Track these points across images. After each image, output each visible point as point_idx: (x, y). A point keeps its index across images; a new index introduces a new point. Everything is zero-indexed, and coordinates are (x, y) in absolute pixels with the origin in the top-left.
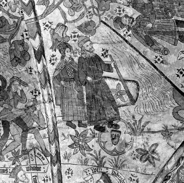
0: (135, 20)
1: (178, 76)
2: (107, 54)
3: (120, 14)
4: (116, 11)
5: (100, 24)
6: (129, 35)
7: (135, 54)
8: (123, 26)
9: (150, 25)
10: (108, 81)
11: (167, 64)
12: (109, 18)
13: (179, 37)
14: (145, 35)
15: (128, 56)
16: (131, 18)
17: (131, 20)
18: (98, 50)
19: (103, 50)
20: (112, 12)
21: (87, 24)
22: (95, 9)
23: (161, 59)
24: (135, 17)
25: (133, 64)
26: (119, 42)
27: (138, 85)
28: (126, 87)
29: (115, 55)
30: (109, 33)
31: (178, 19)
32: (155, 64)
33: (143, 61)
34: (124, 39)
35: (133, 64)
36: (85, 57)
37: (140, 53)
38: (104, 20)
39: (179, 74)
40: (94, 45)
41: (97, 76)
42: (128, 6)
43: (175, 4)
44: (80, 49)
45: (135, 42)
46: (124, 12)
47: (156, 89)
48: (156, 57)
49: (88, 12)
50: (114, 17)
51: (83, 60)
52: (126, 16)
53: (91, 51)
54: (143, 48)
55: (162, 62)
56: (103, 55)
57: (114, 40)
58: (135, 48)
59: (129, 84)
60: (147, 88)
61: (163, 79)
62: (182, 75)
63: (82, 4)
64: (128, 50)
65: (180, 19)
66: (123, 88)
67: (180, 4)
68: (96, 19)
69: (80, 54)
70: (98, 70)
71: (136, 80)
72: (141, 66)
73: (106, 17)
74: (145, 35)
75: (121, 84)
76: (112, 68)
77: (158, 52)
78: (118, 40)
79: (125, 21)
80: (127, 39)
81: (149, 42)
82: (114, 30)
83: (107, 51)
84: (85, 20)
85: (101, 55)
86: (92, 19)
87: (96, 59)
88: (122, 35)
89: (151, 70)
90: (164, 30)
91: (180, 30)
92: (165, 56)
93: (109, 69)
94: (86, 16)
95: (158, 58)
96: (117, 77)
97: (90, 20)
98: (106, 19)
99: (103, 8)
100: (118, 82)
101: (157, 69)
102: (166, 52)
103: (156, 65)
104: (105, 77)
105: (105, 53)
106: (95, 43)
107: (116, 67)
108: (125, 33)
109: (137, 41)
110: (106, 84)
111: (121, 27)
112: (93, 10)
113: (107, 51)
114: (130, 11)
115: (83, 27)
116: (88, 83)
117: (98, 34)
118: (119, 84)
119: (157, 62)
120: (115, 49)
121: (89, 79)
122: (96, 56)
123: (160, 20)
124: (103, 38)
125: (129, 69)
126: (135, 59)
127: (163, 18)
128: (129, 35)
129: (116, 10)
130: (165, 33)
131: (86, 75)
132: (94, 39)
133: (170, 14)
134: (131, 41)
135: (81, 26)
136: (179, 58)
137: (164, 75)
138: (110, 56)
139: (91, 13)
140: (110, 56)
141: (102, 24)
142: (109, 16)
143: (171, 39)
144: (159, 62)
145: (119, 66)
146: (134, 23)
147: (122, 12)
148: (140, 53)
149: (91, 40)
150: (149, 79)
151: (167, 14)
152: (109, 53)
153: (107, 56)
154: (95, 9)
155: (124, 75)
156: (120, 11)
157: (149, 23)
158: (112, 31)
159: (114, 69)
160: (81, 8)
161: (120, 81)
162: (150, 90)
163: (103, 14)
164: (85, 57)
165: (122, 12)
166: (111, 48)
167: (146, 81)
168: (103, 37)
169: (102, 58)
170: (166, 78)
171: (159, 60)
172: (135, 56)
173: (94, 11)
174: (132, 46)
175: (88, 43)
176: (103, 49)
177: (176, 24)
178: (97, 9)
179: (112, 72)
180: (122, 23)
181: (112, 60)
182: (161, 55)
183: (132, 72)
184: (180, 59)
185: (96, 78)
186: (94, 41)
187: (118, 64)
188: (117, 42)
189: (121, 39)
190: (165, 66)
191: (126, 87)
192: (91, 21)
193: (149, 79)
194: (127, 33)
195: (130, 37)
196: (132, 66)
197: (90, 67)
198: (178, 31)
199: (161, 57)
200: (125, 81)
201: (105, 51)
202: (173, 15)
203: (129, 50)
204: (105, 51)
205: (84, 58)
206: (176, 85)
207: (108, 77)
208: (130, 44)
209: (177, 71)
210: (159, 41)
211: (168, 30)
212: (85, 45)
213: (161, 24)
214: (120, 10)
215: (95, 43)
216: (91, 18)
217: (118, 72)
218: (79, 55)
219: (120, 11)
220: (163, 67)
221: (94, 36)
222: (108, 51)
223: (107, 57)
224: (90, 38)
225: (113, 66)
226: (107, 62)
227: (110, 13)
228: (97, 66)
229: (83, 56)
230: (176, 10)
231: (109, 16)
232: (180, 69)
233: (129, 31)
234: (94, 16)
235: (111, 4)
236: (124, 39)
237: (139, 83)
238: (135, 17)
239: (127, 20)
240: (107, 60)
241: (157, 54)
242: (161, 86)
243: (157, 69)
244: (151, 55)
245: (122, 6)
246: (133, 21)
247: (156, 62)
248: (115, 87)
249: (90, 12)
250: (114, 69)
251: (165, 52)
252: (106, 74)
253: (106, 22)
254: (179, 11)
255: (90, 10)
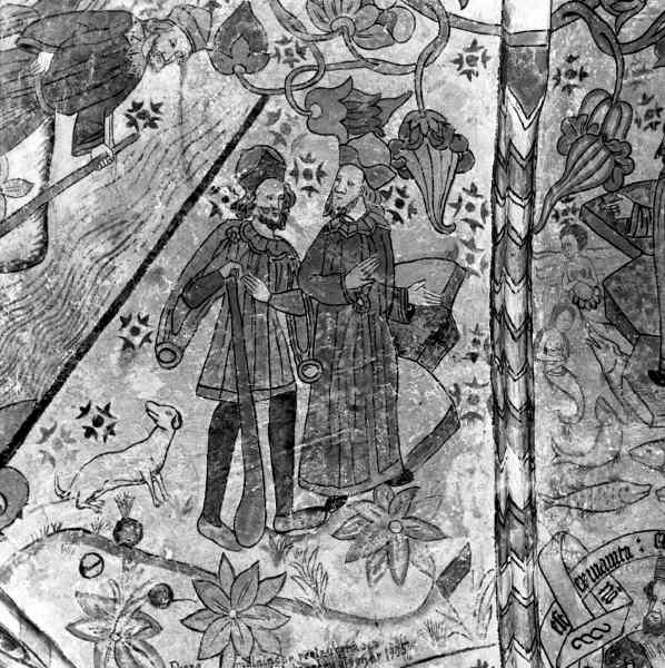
0: (278, 232)
1: (85, 411)
2: (141, 122)
3: (295, 174)
4: (308, 159)
5: (254, 90)
6: (216, 210)
7: (148, 236)
8: (251, 182)
9: (262, 293)
10: (37, 139)
11: (125, 363)
12: (276, 127)
13: (235, 405)
14: (225, 272)
15: (138, 209)
16: (284, 217)
17: (276, 219)
18: (156, 86)
19: (156, 108)
20: (297, 144)
21: (255, 41)
22: (311, 74)
23: (137, 340)
24: (287, 233)
25: (109, 233)
26: (187, 171)
27: (31, 264)
28: (21, 215)
29: (137, 156)
30: (219, 129)
31: (299, 402)
32: (117, 317)
33: (125, 269)
34: (200, 190)
35: (109, 233)
36: (129, 35)
37: (152, 256)
38: (270, 107)
39: (94, 413)
40: (174, 69)
41: (55, 92)
42: (328, 210)
43: (354, 390)
44: (161, 15)
45: (195, 231)
46: (305, 193)
47: (26, 336)
48: (144, 321)
49: (301, 45)
50: (281, 149)
51: (120, 29)
52: (289, 200)
53: (154, 60)
54: (172, 264)
55: (128, 345)
56: (137, 106)
57: (193, 149)
58: (169, 233)
59: (32, 227)
60: (23, 303)
61: (65, 356)
62: (90, 424)
63: (336, 25)
64: (159, 207)
65: (301, 411)
66: (15, 204)
67: (354, 408)
68: (272, 75)
69: (145, 17)
70: (79, 94)
71: (50, 254)
72: (105, 266)
73: (283, 118)
74: (225, 272)
75: (28, 198)
76: (88, 151)
77: (162, 327)
78: (194, 167)
79: (269, 193)
80: (203, 200)
81: (196, 291)
82: (231, 147)
83: (152, 124)
84: (274, 32)
85: (138, 101)
86: (273, 61)
87: (118, 79)
88: (217, 181)
89: (92, 306)
90: (250, 347)
91: (258, 407)
92: (151, 355)
93: (87, 138)
94: (289, 36)
95: (143, 328)
96: (58, 174)
97: (271, 50)
98: (274, 117)
99: (316, 110)
100: (38, 182)
101: (99, 329)
102: (166, 356)
103: (116, 321)
104: (52, 126)
105: (144, 117)
106: (183, 72)
107: (95, 164)
108: (224, 192)
109: (197, 241)
110: (26, 132)
111: (244, 176)
112: (310, 68)
113: (152, 124)
114: (308, 218)
115: (247, 25)
116: (27, 56)
117: (217, 82)
118: (30, 185)
119: (124, 326)
120: (159, 155)
121: (45, 60)
122: (134, 81)
123: (286, 331)
124: (200, 107)
125: (89, 220)
126: (129, 237)
127: (295, 344)
128: (216, 210)
129: (312, 162)
130: (237, 346)
131: (57, 43)
132: (198, 71)
133: (312, 371)
134: (195, 219)
135: (251, 17)
136: (152, 407)
137: (79, 356)
138: (134, 138)
139: (297, 56)
140: (134, 138)
141: (254, 99)
142: (286, 129)
143: (220, 375)
144: (126, 332)
145: (95, 179)
146: (263, 229)
147: (304, 182)
148: (152, 256)
149: (194, 55)
150: (60, 302)
151: (316, 360)
152: (146, 134)
153: (132, 123)
154: (311, 74)
155: (65, 203)
156: (307, 175)
157: (269, 287)
158: (228, 140)
159: (84, 160)
160: (321, 19)
161: (42, 191)
162: (20, 316)
163: (295, 106)
164: (129, 35)
165: (304, 182)
166: (164, 138)
167: (49, 293)
168: (207, 105)
169: (127, 105)
170: (70, 367)
171: (135, 331)
172: (140, 235)
173: (303, 70)
174: (176, 222)
175: (184, 46)
176: (160, 105)
177: (282, 391)
178: (313, 82)
179: (74, 154)
180: (261, 180)
181: (119, 148)
182: (153, 337)
183: (80, 231)
184: (148, 410)
185: (49, 88)
186: (190, 69)
187: (103, 176)
188: (188, 159)
189: (199, 177)
190: (114, 358)
191: (21, 215)
192: (267, 58)
193: (60, 302)
194: (226, 200)
195: (208, 212)
196: (101, 227)
197: (92, 61)
198: (253, 402)
199: (147, 339)
200: (42, 207)
201: (153, 114)
202: (314, 383)
203: (160, 212)
204: (153, 114)
205: (127, 31)
206: (50, 408)
207: (52, 140)
208: (183, 212)
209: (102, 407)
210: (207, 327)
211: (251, 362)
212: (177, 33)
213: (272, 337)
214: (311, 177)
215: (183, 72)
216: (278, 55)
217: (76, 176)
218: (142, 13)
219: (307, 175)
220: (108, 348)
221: (211, 68)
222: (154, 126)
223: (130, 125)
224: (203, 54)
225: (97, 152)
226: (112, 128)
227: (295, 132)
228: (96, 87)
229: (136, 28)
230: (333, 396)
231: (286, 129)
232: (110, 416)
233: (233, 207)
234: (285, 70)
235: (333, 143)
236: (200, 190)
237: (39, 268)
238: (287, 233)
239: (274, 203)
240: (119, 127)
241: (154, 319)
242: (38, 355)
243: (99, 329)
244: (149, 301)
245: (326, 186)
246: (272, 226)
247: (125, 322)
248: (15, 173)
249: (301, 52)
250: (84, 160)
251: (169, 355)
252: (66, 125)
253: (262, 117)
254: (330, 405)
255: (308, 53)
